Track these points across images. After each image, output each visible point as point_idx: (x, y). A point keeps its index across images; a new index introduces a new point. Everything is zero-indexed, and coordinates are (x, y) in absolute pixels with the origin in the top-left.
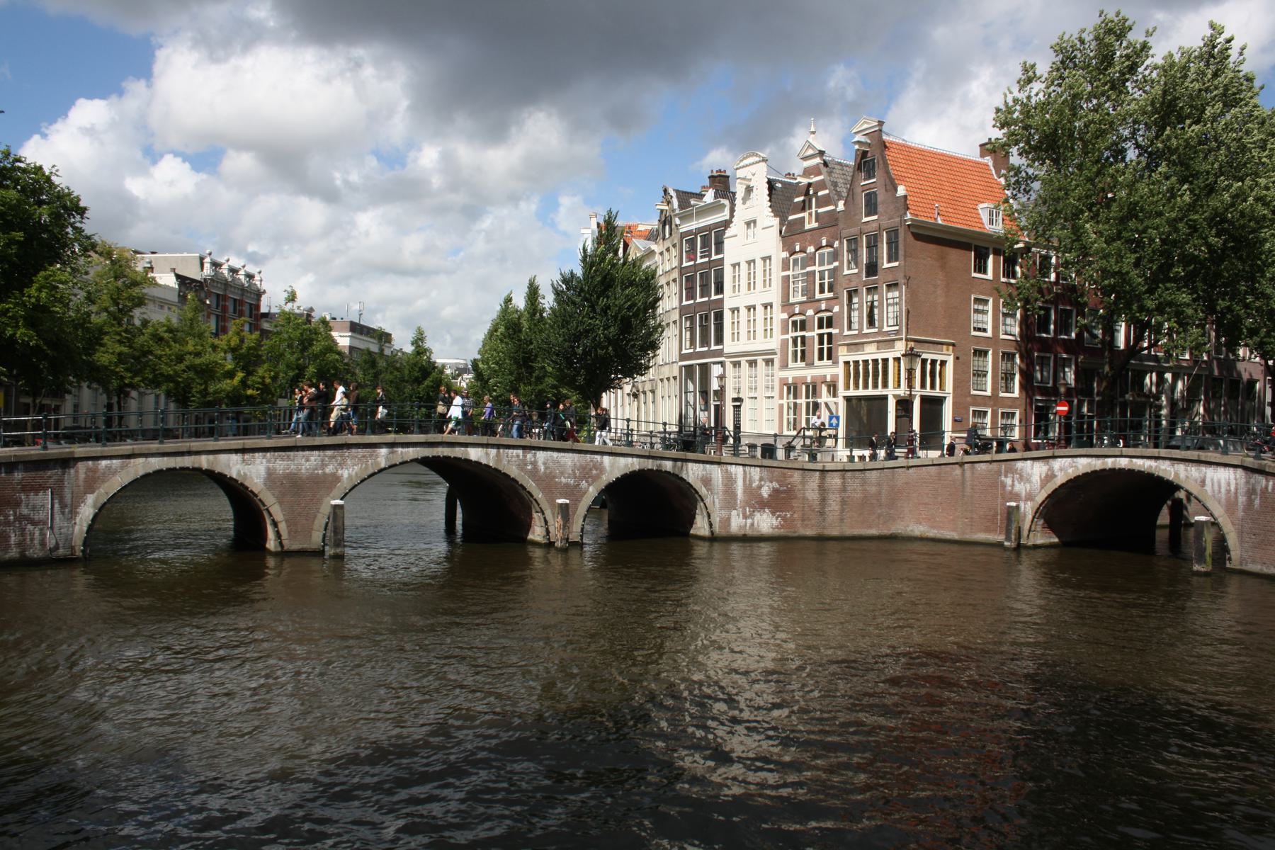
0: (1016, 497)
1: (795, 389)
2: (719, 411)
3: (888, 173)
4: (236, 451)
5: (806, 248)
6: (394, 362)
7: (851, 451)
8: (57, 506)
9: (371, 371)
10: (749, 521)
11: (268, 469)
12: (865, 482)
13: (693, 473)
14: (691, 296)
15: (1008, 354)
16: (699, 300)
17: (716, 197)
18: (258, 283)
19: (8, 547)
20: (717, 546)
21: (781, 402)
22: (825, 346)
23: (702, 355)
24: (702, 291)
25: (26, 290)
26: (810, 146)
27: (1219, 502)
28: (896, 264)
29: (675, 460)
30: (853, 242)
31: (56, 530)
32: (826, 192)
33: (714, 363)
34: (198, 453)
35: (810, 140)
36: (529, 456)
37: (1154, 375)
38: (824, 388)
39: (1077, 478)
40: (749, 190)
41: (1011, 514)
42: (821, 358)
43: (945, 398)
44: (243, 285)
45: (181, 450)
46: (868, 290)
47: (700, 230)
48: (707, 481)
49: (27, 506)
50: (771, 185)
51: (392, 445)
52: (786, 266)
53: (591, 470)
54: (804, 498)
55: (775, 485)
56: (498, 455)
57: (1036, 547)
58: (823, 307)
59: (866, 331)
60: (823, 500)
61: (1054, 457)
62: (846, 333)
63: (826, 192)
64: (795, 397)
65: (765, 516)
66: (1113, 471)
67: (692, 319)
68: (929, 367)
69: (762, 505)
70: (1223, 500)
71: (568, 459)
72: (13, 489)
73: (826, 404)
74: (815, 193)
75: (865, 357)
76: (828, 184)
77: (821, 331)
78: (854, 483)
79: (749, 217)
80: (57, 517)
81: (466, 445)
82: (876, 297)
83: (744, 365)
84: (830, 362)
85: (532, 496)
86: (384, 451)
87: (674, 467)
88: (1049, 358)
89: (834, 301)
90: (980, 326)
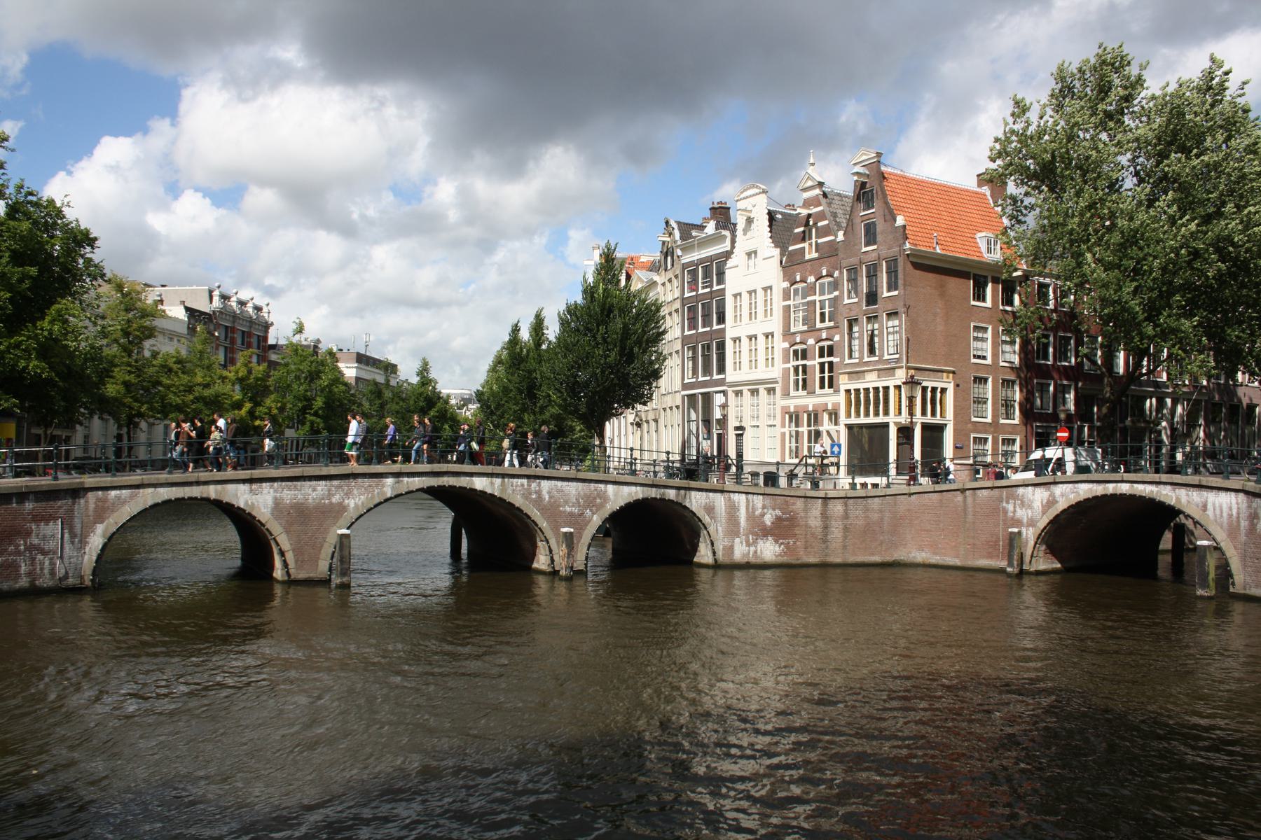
0: (1018, 523)
1: (797, 417)
2: (721, 438)
3: (886, 203)
4: (244, 481)
5: (806, 278)
6: (399, 393)
7: (853, 479)
8: (67, 536)
9: (378, 402)
10: (752, 549)
11: (276, 498)
12: (868, 510)
13: (696, 501)
14: (693, 326)
15: (1008, 381)
16: (701, 330)
17: (717, 229)
18: (266, 315)
19: (18, 576)
20: (720, 573)
21: (783, 430)
22: (827, 375)
23: (704, 384)
24: (704, 321)
25: (39, 323)
26: (810, 178)
27: (1222, 527)
28: (896, 293)
29: (678, 488)
30: (853, 272)
31: (66, 560)
32: (826, 222)
33: (717, 392)
34: (207, 483)
35: (810, 171)
36: (534, 485)
37: (1154, 400)
38: (826, 416)
39: (1079, 504)
40: (750, 221)
41: (1013, 540)
42: (822, 387)
43: (946, 425)
44: (251, 317)
45: (190, 480)
46: (869, 318)
47: (701, 261)
48: (710, 509)
49: (37, 535)
50: (771, 216)
51: (398, 475)
52: (786, 295)
53: (595, 498)
54: (807, 526)
55: (778, 512)
56: (503, 484)
57: (1038, 573)
58: (824, 336)
59: (866, 359)
60: (826, 528)
61: (1055, 483)
62: (847, 361)
63: (826, 222)
64: (797, 426)
65: (768, 544)
66: (1113, 496)
67: (694, 349)
68: (929, 394)
69: (765, 532)
70: (1225, 525)
71: (572, 488)
72: (24, 519)
73: (828, 432)
74: (815, 224)
75: (866, 386)
76: (828, 215)
77: (822, 360)
78: (856, 510)
79: (751, 248)
80: (67, 546)
81: (471, 474)
82: (876, 326)
83: (746, 394)
84: (831, 391)
85: (537, 525)
86: (390, 481)
87: (677, 495)
88: (1049, 385)
89: (834, 330)
90: (980, 353)
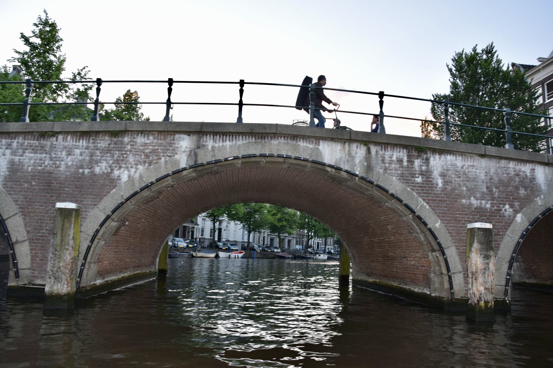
11: (12, 163)
53: (517, 188)
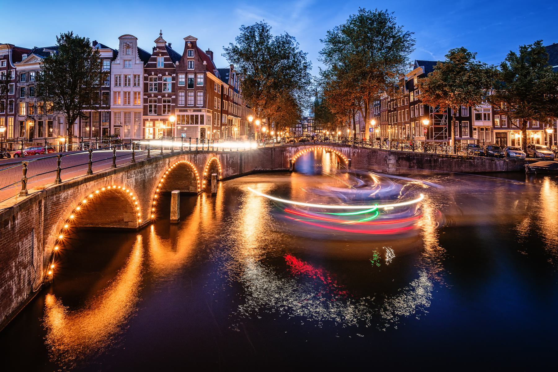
11: (136, 179)
52: (146, 79)
